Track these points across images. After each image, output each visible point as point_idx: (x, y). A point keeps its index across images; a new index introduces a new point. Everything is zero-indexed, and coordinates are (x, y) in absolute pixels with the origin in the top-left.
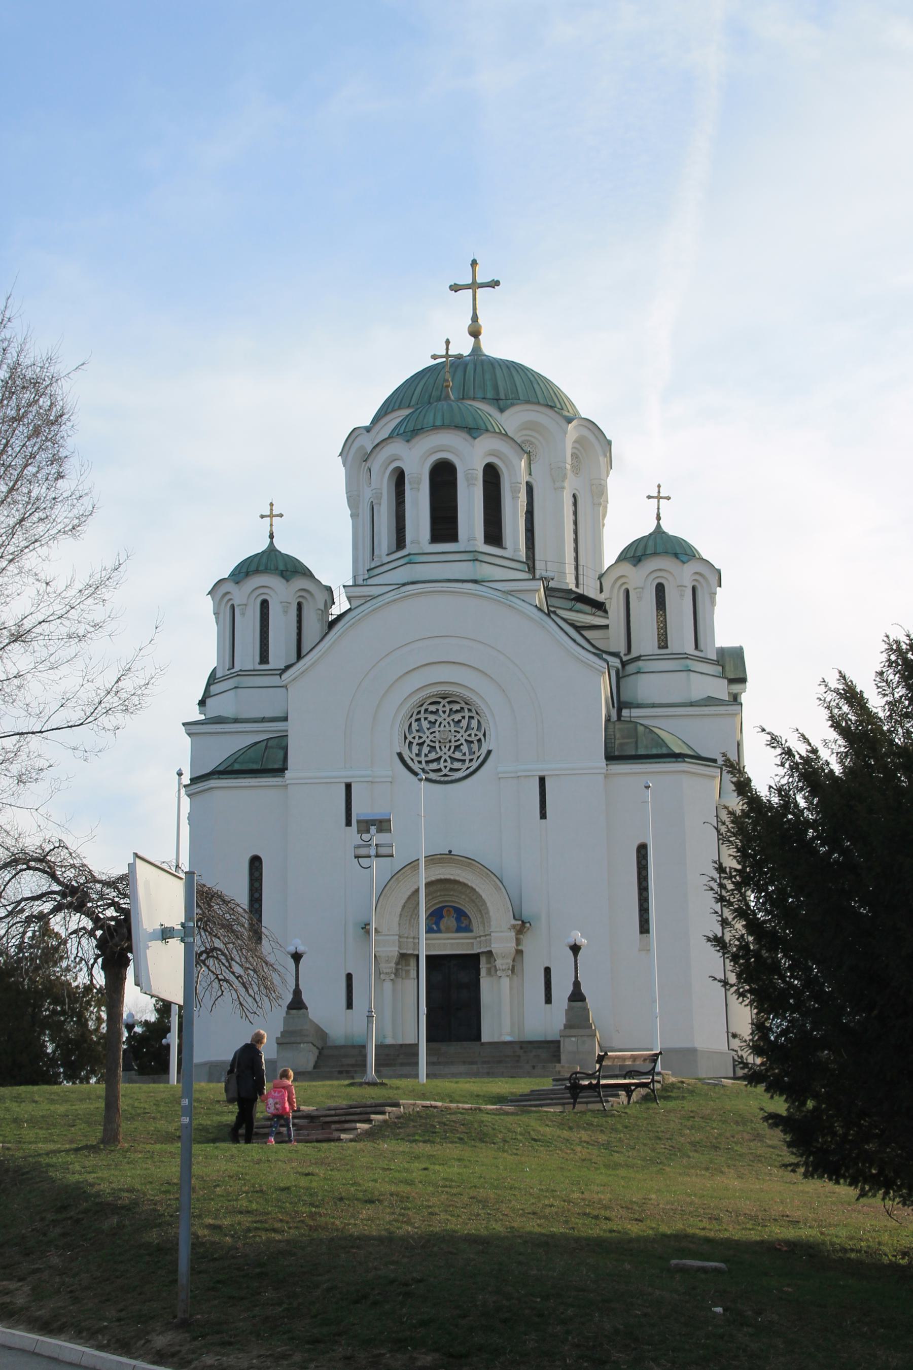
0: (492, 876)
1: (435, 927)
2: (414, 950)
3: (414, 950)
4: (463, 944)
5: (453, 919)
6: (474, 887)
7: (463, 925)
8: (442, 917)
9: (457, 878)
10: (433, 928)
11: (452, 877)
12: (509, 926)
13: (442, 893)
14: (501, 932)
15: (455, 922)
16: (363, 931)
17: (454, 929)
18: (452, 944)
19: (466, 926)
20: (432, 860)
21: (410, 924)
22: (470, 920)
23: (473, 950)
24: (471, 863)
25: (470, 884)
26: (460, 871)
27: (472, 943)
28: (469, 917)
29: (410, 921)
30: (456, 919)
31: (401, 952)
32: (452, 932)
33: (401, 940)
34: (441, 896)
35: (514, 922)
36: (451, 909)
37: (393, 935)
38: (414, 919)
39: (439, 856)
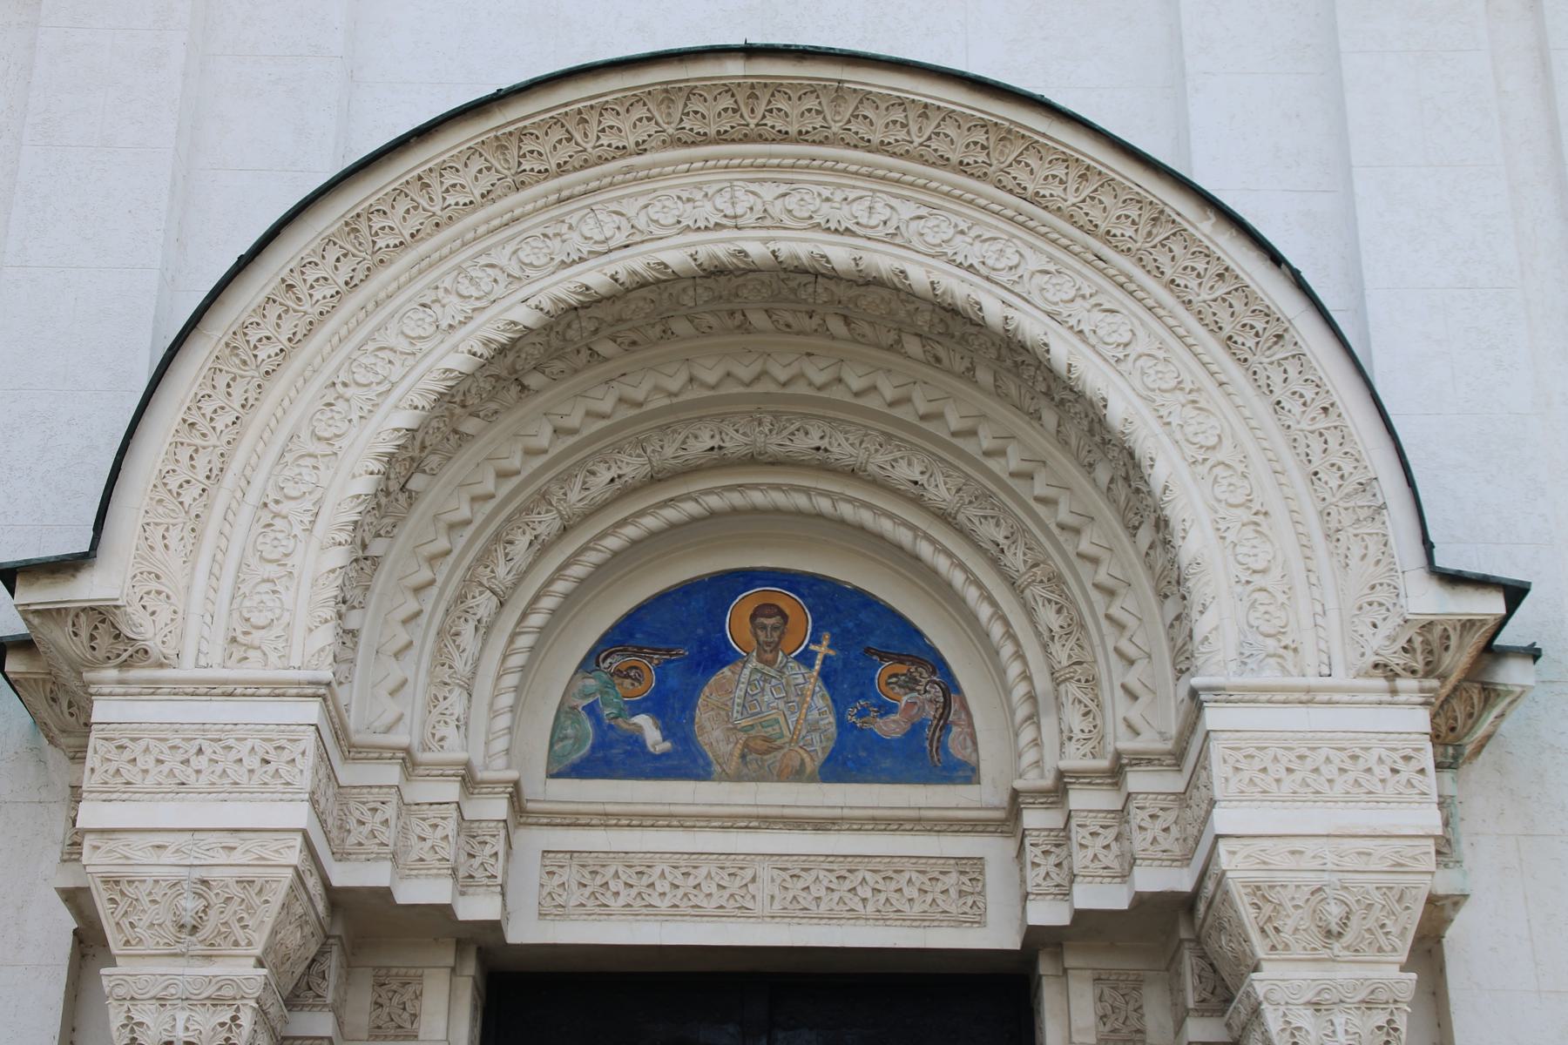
0: (1206, 227)
1: (649, 729)
2: (465, 883)
3: (465, 883)
4: (890, 867)
5: (808, 680)
6: (1031, 326)
7: (891, 727)
8: (715, 656)
9: (882, 260)
10: (636, 741)
11: (840, 255)
12: (1381, 643)
13: (735, 442)
14: (1308, 698)
15: (819, 706)
16: (68, 790)
17: (820, 746)
18: (792, 867)
19: (916, 729)
20: (668, 93)
21: (440, 659)
22: (950, 686)
23: (981, 923)
24: (1007, 135)
25: (993, 311)
26: (907, 210)
27: (972, 867)
28: (938, 665)
29: (448, 635)
30: (826, 676)
31: (343, 876)
32: (797, 775)
33: (348, 774)
34: (720, 462)
35: (1430, 601)
36: (788, 601)
37: (278, 691)
38: (485, 630)
39: (734, 68)
